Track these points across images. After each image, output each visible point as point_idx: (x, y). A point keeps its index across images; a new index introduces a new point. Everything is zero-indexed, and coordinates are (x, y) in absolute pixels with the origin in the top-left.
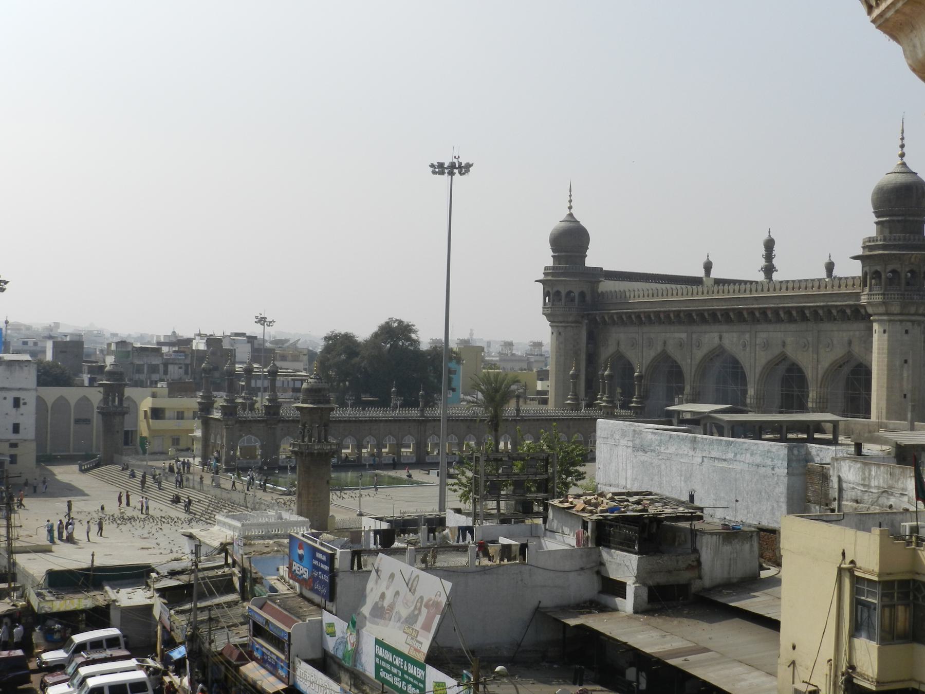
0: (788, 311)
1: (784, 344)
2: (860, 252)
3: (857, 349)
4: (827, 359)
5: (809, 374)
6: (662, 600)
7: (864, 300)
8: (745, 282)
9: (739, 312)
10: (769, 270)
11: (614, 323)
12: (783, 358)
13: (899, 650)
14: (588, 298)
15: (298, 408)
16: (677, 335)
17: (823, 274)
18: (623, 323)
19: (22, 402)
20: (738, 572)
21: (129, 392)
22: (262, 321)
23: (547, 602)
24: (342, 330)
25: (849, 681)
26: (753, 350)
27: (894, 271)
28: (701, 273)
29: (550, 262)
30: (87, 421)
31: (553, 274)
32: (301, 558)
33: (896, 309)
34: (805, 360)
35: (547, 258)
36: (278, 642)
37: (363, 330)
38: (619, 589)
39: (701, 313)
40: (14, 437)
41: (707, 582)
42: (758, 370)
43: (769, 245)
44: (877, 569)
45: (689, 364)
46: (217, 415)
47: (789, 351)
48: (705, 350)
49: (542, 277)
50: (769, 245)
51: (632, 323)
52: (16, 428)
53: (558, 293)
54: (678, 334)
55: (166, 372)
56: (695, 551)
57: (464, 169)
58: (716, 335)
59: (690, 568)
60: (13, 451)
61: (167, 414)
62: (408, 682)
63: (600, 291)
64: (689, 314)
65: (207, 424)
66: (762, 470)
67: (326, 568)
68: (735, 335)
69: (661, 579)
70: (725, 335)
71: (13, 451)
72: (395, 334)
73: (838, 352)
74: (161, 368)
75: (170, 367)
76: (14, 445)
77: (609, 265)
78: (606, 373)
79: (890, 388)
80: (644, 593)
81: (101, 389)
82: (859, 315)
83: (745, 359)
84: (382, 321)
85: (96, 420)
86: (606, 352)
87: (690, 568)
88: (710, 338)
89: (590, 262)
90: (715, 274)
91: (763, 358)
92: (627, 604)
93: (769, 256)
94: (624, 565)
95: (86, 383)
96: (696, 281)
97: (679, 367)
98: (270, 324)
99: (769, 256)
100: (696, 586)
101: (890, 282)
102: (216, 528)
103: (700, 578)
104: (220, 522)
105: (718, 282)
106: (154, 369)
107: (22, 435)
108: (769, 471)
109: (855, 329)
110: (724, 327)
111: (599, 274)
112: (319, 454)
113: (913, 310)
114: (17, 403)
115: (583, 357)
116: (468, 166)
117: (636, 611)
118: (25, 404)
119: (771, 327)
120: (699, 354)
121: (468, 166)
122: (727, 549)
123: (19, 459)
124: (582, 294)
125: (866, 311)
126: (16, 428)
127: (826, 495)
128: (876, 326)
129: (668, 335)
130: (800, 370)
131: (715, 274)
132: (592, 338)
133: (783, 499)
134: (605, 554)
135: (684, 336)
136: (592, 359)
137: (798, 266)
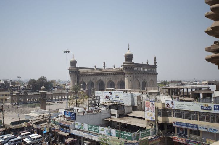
0: (111, 73)
1: (111, 79)
2: (123, 64)
3: (122, 79)
4: (118, 81)
5: (115, 84)
6: (121, 116)
7: (124, 71)
8: (101, 69)
9: (103, 74)
10: (104, 67)
11: (82, 76)
12: (111, 81)
13: (164, 117)
14: (77, 72)
15: (41, 92)
16: (93, 78)
17: (113, 67)
18: (83, 76)
20: (129, 112)
22: (19, 77)
23: (103, 117)
24: (32, 78)
25: (158, 122)
26: (106, 80)
27: (128, 67)
28: (94, 67)
29: (70, 66)
31: (71, 68)
32: (67, 114)
33: (129, 73)
34: (114, 81)
35: (69, 65)
36: (68, 128)
37: (36, 79)
38: (114, 115)
39: (97, 74)
41: (126, 113)
42: (107, 83)
43: (104, 63)
44: (161, 107)
45: (95, 83)
46: (15, 95)
47: (112, 80)
48: (98, 80)
49: (69, 69)
50: (104, 63)
51: (85, 76)
53: (72, 71)
54: (93, 78)
56: (124, 109)
57: (69, 52)
58: (99, 78)
59: (124, 111)
62: (95, 130)
63: (79, 70)
64: (95, 74)
65: (12, 96)
66: (127, 97)
67: (74, 115)
68: (103, 78)
69: (120, 113)
70: (101, 78)
72: (42, 79)
73: (119, 80)
77: (80, 67)
78: (82, 84)
79: (128, 85)
80: (118, 115)
82: (123, 74)
83: (104, 81)
84: (40, 77)
86: (80, 81)
87: (124, 111)
88: (98, 78)
89: (77, 66)
90: (96, 68)
91: (107, 81)
92: (116, 117)
93: (104, 65)
94: (115, 112)
96: (94, 69)
97: (92, 82)
98: (20, 78)
99: (104, 65)
100: (125, 114)
101: (128, 69)
102: (31, 113)
103: (125, 113)
104: (32, 112)
105: (97, 69)
108: (128, 97)
109: (122, 76)
110: (100, 76)
111: (78, 68)
112: (45, 100)
113: (131, 73)
115: (76, 82)
116: (70, 51)
117: (118, 118)
119: (108, 76)
120: (97, 81)
121: (70, 51)
122: (128, 108)
124: (76, 71)
125: (124, 73)
127: (141, 100)
128: (126, 76)
129: (91, 78)
130: (113, 83)
131: (96, 68)
132: (77, 78)
133: (130, 101)
134: (111, 110)
135: (94, 78)
136: (78, 83)
137: (109, 66)
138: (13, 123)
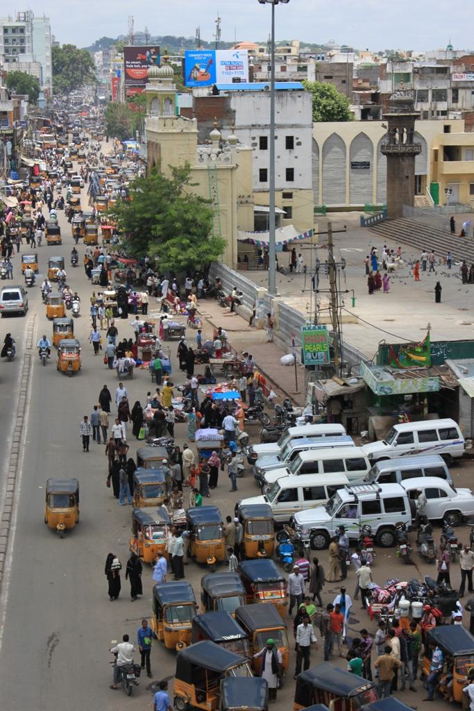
19: (295, 141)
21: (419, 126)
30: (366, 165)
40: (287, 186)
52: (290, 175)
55: (455, 99)
60: (288, 202)
61: (463, 155)
71: (288, 202)
74: (450, 95)
75: (461, 93)
76: (288, 196)
81: (386, 123)
85: (380, 165)
95: (358, 116)
106: (439, 95)
107: (299, 181)
114: (290, 143)
118: (299, 144)
123: (294, 212)
126: (290, 175)
138: (390, 355)
